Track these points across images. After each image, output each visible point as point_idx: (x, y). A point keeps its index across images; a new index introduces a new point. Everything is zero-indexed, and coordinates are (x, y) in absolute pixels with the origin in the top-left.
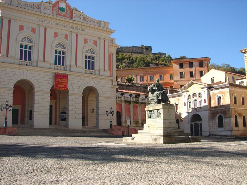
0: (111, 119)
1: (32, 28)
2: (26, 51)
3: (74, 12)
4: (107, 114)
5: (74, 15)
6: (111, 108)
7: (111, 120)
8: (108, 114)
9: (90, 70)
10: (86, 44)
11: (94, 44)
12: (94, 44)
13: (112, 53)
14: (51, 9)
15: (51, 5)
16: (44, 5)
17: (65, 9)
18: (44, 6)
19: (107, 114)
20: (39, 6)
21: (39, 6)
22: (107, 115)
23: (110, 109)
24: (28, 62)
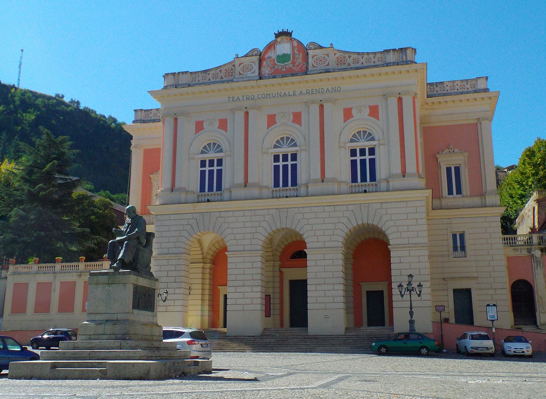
0: (411, 305)
1: (220, 121)
2: (211, 172)
3: (311, 53)
4: (401, 292)
5: (310, 60)
6: (411, 276)
7: (411, 308)
8: (403, 293)
9: (356, 184)
10: (347, 122)
11: (370, 115)
12: (370, 115)
13: (479, 119)
14: (256, 67)
15: (256, 59)
16: (240, 64)
17: (290, 54)
18: (242, 65)
19: (401, 292)
20: (232, 69)
21: (232, 69)
22: (402, 296)
23: (406, 279)
24: (208, 195)
